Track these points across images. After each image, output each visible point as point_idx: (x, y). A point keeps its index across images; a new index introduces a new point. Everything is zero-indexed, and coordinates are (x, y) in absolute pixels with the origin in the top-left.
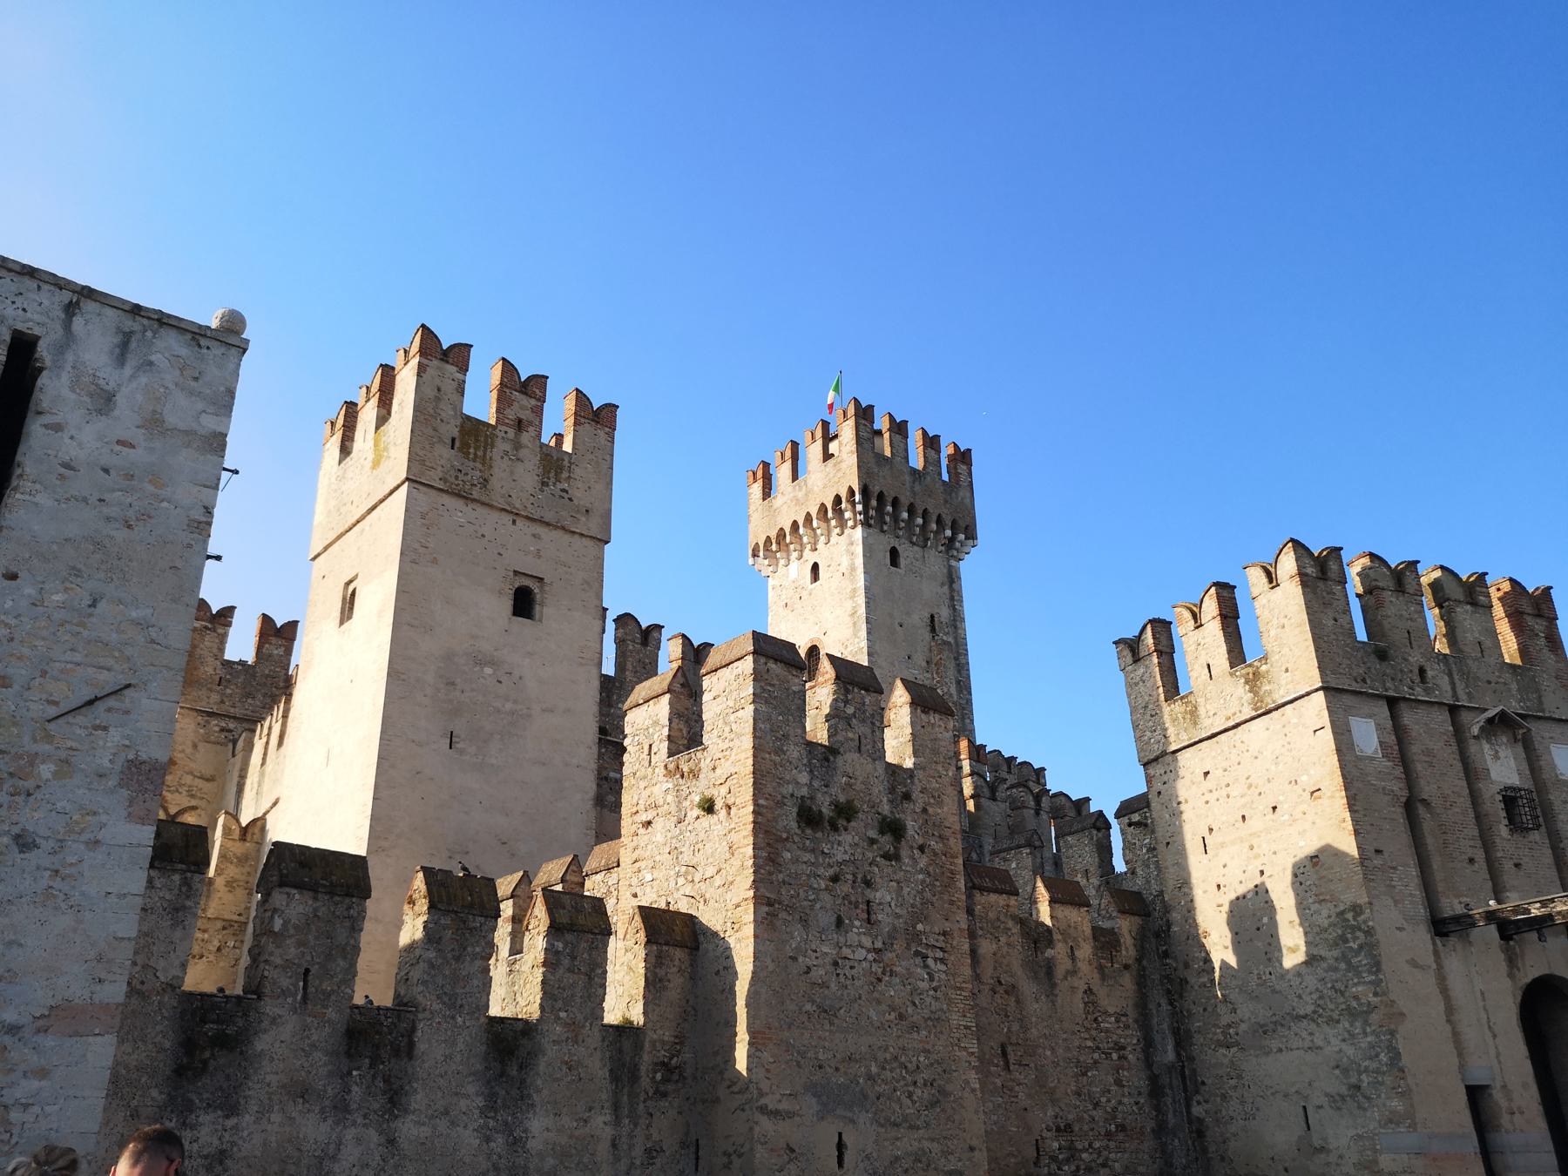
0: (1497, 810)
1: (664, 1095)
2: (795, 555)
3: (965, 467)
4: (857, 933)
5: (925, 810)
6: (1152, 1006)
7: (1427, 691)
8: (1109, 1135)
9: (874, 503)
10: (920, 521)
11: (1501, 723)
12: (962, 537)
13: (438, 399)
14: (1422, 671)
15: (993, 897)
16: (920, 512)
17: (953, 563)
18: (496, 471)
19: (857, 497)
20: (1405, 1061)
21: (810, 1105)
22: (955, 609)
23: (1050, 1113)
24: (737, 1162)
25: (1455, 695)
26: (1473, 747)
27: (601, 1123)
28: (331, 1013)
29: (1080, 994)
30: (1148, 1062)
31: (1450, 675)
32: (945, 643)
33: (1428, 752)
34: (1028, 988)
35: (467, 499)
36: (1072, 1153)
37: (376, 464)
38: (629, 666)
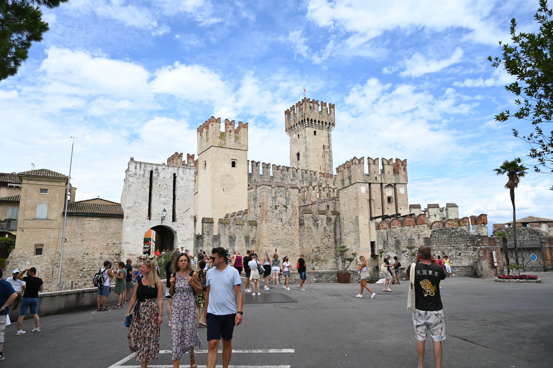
0: (386, 200)
1: (253, 244)
2: (295, 132)
3: (333, 109)
4: (280, 223)
5: (292, 204)
6: (337, 229)
7: (376, 181)
8: (326, 248)
9: (310, 122)
10: (321, 124)
11: (390, 185)
12: (331, 126)
13: (216, 130)
14: (376, 178)
15: (308, 214)
16: (321, 122)
17: (329, 132)
18: (227, 141)
19: (306, 121)
20: (360, 238)
21: (272, 245)
22: (329, 143)
23: (316, 245)
24: (262, 252)
25: (382, 181)
26: (384, 190)
27: (244, 247)
28: (211, 236)
29: (323, 228)
30: (335, 238)
31: (381, 178)
32: (327, 152)
33: (375, 191)
34: (313, 227)
35: (223, 147)
36: (319, 251)
37: (207, 141)
38: (254, 171)
